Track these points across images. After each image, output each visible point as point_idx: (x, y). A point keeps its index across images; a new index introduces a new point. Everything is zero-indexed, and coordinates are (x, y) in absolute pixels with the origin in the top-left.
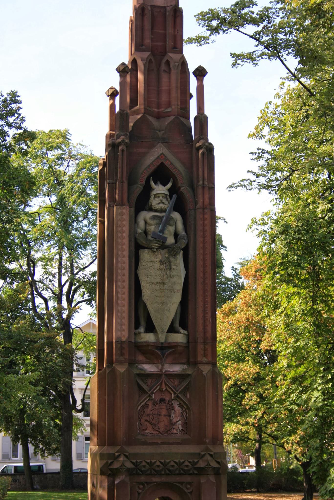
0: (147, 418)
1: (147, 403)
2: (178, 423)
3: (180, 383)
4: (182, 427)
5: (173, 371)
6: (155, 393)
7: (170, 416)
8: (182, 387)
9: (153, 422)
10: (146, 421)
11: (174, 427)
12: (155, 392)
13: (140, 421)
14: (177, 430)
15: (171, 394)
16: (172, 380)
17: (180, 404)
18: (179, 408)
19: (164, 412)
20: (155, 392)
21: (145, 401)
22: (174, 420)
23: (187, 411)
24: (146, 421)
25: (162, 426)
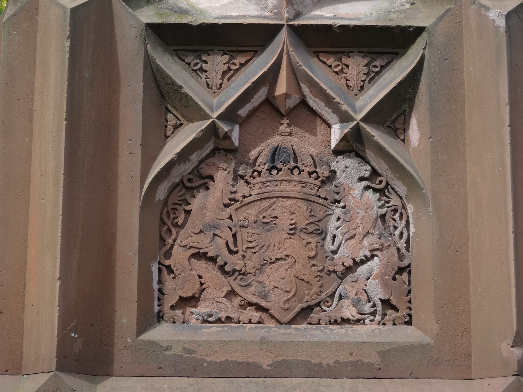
0: (203, 242)
1: (206, 171)
2: (362, 270)
3: (372, 77)
4: (385, 286)
5: (335, 18)
6: (243, 123)
7: (322, 233)
8: (386, 86)
9: (235, 262)
10: (200, 255)
11: (345, 287)
12: (243, 112)
13: (168, 255)
14: (357, 303)
15: (329, 126)
16: (331, 61)
17: (375, 173)
18: (369, 193)
19: (289, 212)
20: (243, 112)
21: (195, 158)
22: (346, 254)
23: (410, 208)
24: (200, 255)
25: (276, 283)
